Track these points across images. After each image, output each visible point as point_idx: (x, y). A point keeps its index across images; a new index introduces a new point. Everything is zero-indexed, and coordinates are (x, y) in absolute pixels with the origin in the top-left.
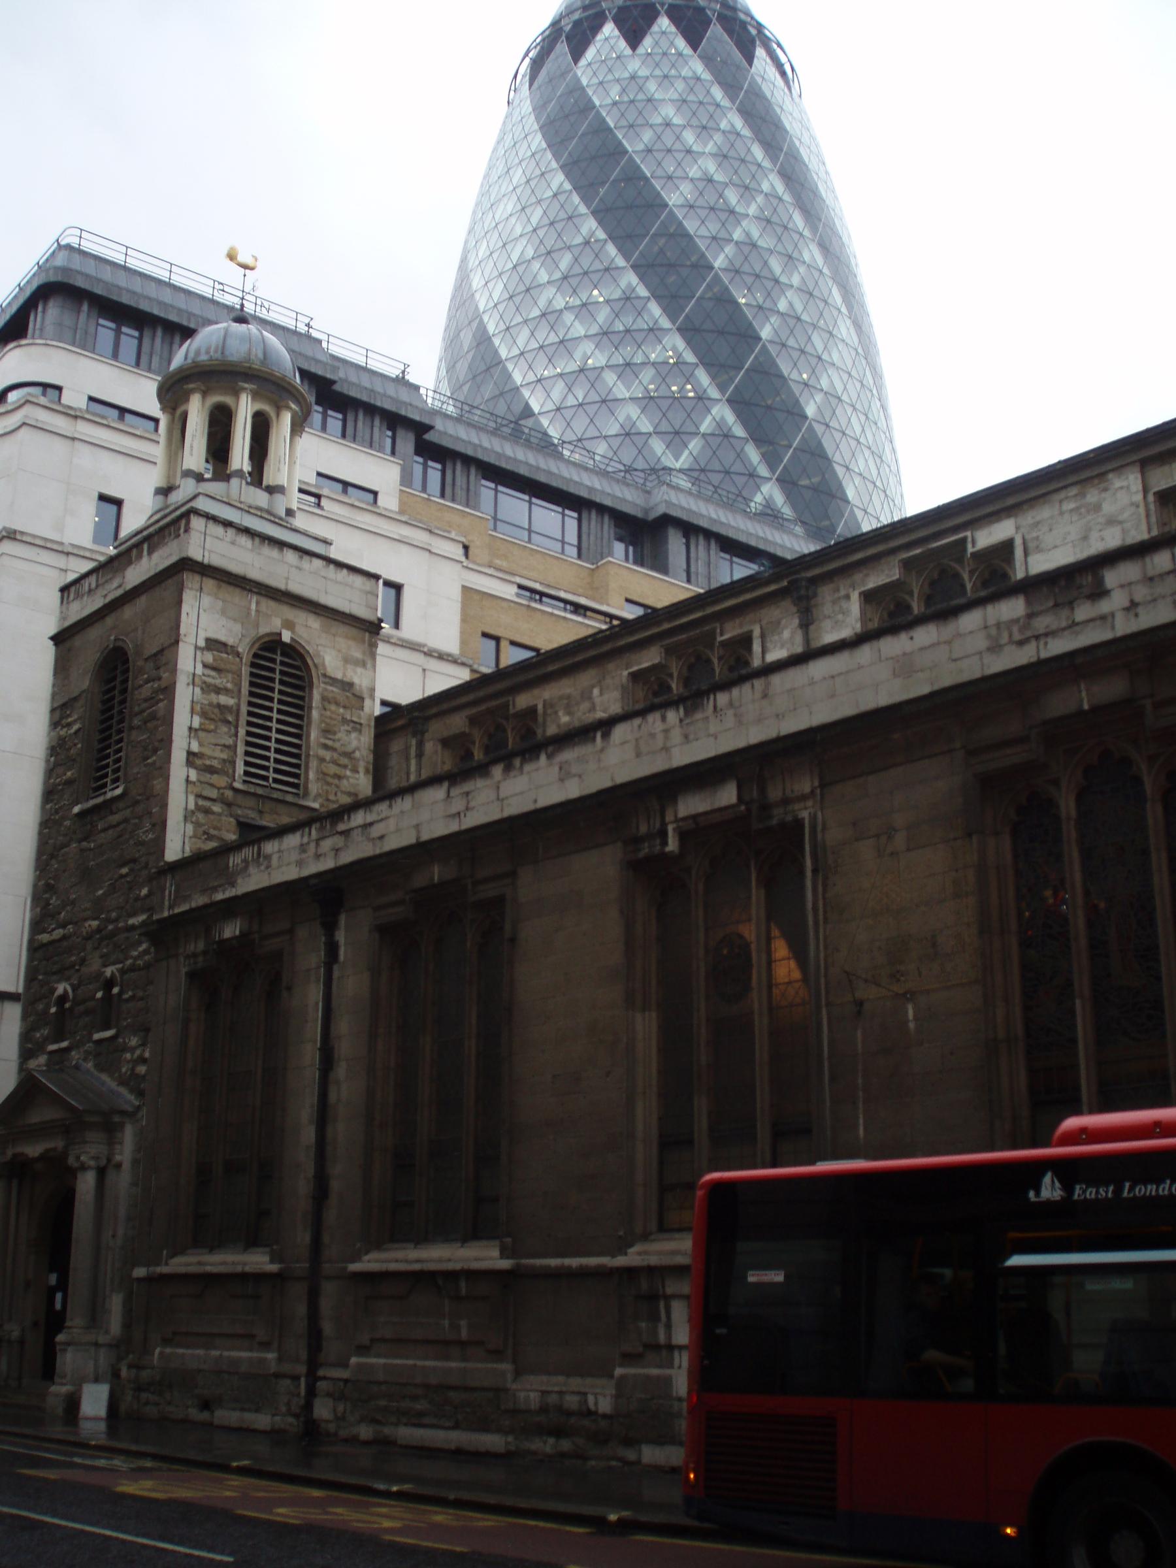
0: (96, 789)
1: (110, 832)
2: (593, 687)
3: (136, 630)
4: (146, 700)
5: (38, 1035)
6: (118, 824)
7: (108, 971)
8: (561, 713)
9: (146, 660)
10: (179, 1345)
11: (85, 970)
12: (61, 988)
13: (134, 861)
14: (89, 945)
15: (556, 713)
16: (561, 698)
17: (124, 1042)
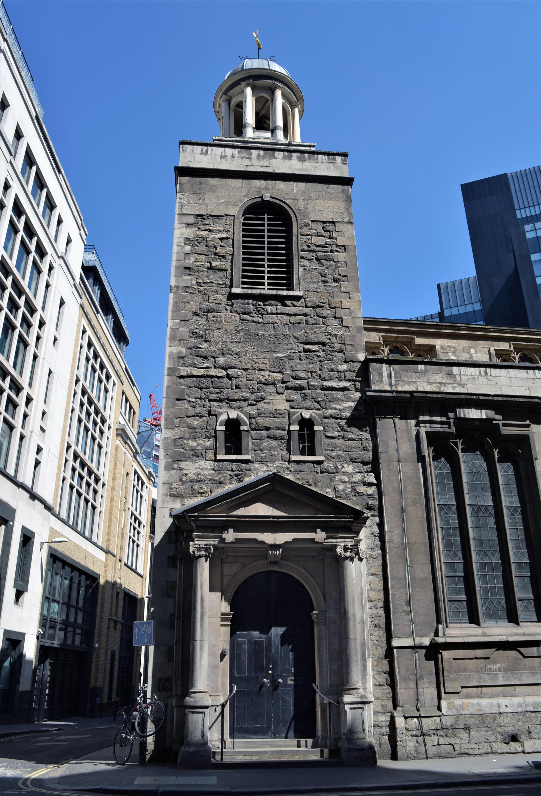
0: (244, 283)
1: (285, 317)
2: (470, 348)
3: (297, 200)
4: (317, 246)
5: (194, 444)
6: (296, 315)
7: (307, 415)
8: (450, 354)
9: (312, 221)
10: (468, 696)
11: (261, 405)
12: (233, 414)
13: (324, 344)
14: (271, 389)
15: (447, 353)
16: (449, 347)
17: (336, 467)
